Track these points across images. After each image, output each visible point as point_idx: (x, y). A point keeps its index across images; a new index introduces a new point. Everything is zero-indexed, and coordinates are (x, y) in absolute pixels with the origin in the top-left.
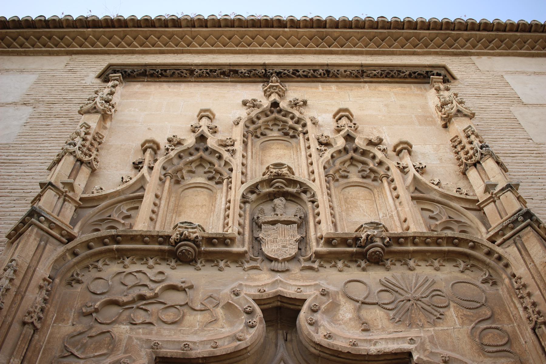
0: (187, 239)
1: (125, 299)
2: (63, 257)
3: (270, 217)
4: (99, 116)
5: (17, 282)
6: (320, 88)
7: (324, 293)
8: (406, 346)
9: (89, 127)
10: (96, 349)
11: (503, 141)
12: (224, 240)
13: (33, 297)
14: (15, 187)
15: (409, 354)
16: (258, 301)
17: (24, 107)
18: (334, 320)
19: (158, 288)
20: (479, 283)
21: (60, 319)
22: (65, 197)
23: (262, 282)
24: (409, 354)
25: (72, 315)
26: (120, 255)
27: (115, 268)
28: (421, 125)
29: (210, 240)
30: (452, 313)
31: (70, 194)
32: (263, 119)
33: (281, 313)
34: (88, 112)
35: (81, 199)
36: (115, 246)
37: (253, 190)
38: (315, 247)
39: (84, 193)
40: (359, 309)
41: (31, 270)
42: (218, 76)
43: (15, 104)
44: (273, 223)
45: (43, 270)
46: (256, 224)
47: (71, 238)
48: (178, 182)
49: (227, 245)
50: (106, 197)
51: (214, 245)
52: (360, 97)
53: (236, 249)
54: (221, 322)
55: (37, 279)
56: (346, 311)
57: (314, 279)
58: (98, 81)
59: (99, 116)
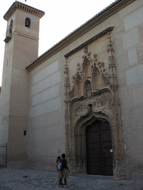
1: (77, 109)
2: (70, 104)
3: (88, 89)
4: (66, 74)
5: (66, 112)
7: (94, 102)
8: (101, 110)
9: (65, 78)
12: (83, 97)
13: (69, 112)
16: (88, 105)
19: (79, 105)
21: (73, 113)
22: (67, 95)
24: (101, 112)
26: (75, 101)
27: (76, 103)
29: (81, 97)
30: (107, 102)
31: (68, 94)
32: (86, 61)
33: (90, 105)
34: (64, 73)
35: (69, 93)
37: (85, 84)
38: (93, 95)
39: (69, 91)
40: (98, 104)
41: (67, 109)
42: (78, 50)
43: (58, 70)
44: (88, 90)
45: (69, 108)
46: (87, 91)
47: (70, 101)
48: (79, 83)
50: (71, 92)
53: (85, 97)
55: (69, 110)
59: (66, 74)
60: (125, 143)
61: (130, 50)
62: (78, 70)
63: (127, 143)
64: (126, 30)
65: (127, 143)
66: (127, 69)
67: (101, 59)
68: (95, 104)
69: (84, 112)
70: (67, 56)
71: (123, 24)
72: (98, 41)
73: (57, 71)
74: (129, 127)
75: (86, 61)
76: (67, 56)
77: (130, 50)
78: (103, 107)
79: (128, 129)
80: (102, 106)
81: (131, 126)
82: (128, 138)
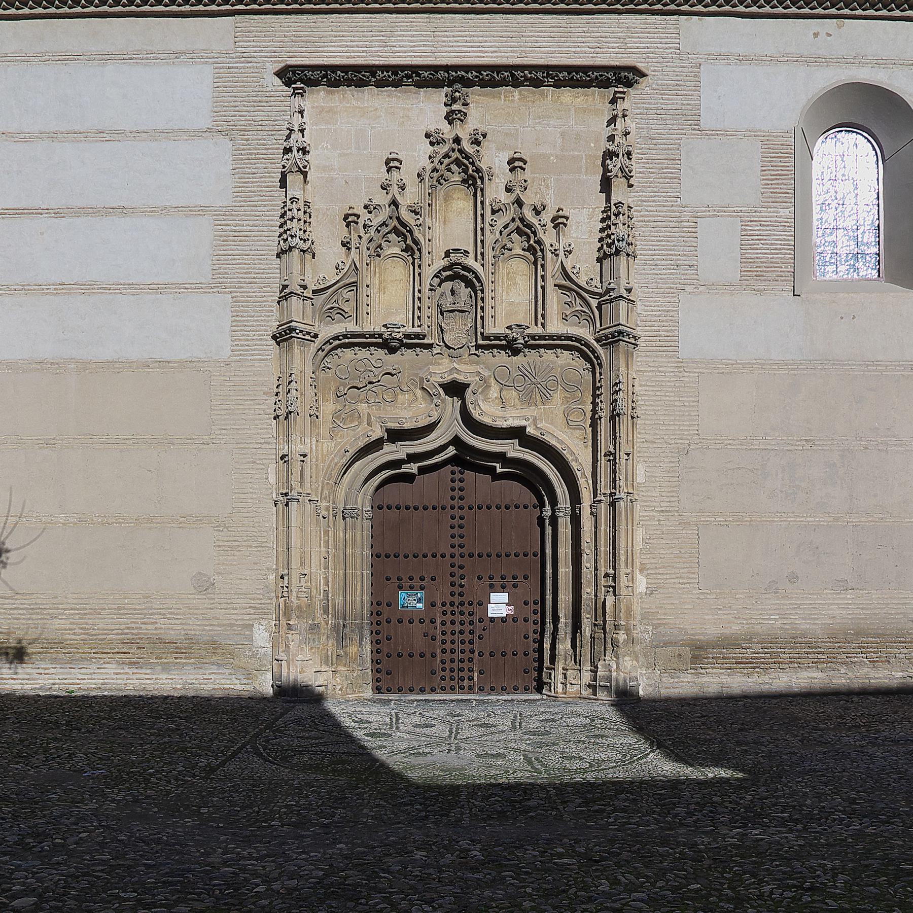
0: (394, 339)
6: (503, 97)
8: (523, 423)
10: (352, 421)
11: (654, 201)
12: (417, 336)
14: (257, 271)
15: (525, 428)
17: (221, 139)
18: (486, 399)
20: (581, 371)
23: (442, 369)
24: (525, 428)
25: (332, 396)
27: (348, 353)
28: (586, 173)
30: (558, 396)
33: (455, 389)
36: (347, 341)
43: (209, 130)
49: (420, 339)
51: (412, 339)
52: (539, 118)
53: (426, 341)
54: (420, 399)
56: (494, 392)
57: (477, 363)
58: (277, 81)
60: (641, 571)
61: (709, 216)
62: (395, 190)
63: (649, 572)
64: (707, 122)
65: (649, 572)
66: (688, 289)
67: (551, 191)
68: (488, 387)
69: (411, 411)
70: (297, 77)
71: (697, 88)
72: (544, 96)
73: (198, 134)
74: (667, 511)
75: (446, 161)
76: (297, 77)
77: (709, 216)
78: (531, 412)
79: (659, 520)
80: (530, 404)
81: (677, 511)
82: (662, 551)
